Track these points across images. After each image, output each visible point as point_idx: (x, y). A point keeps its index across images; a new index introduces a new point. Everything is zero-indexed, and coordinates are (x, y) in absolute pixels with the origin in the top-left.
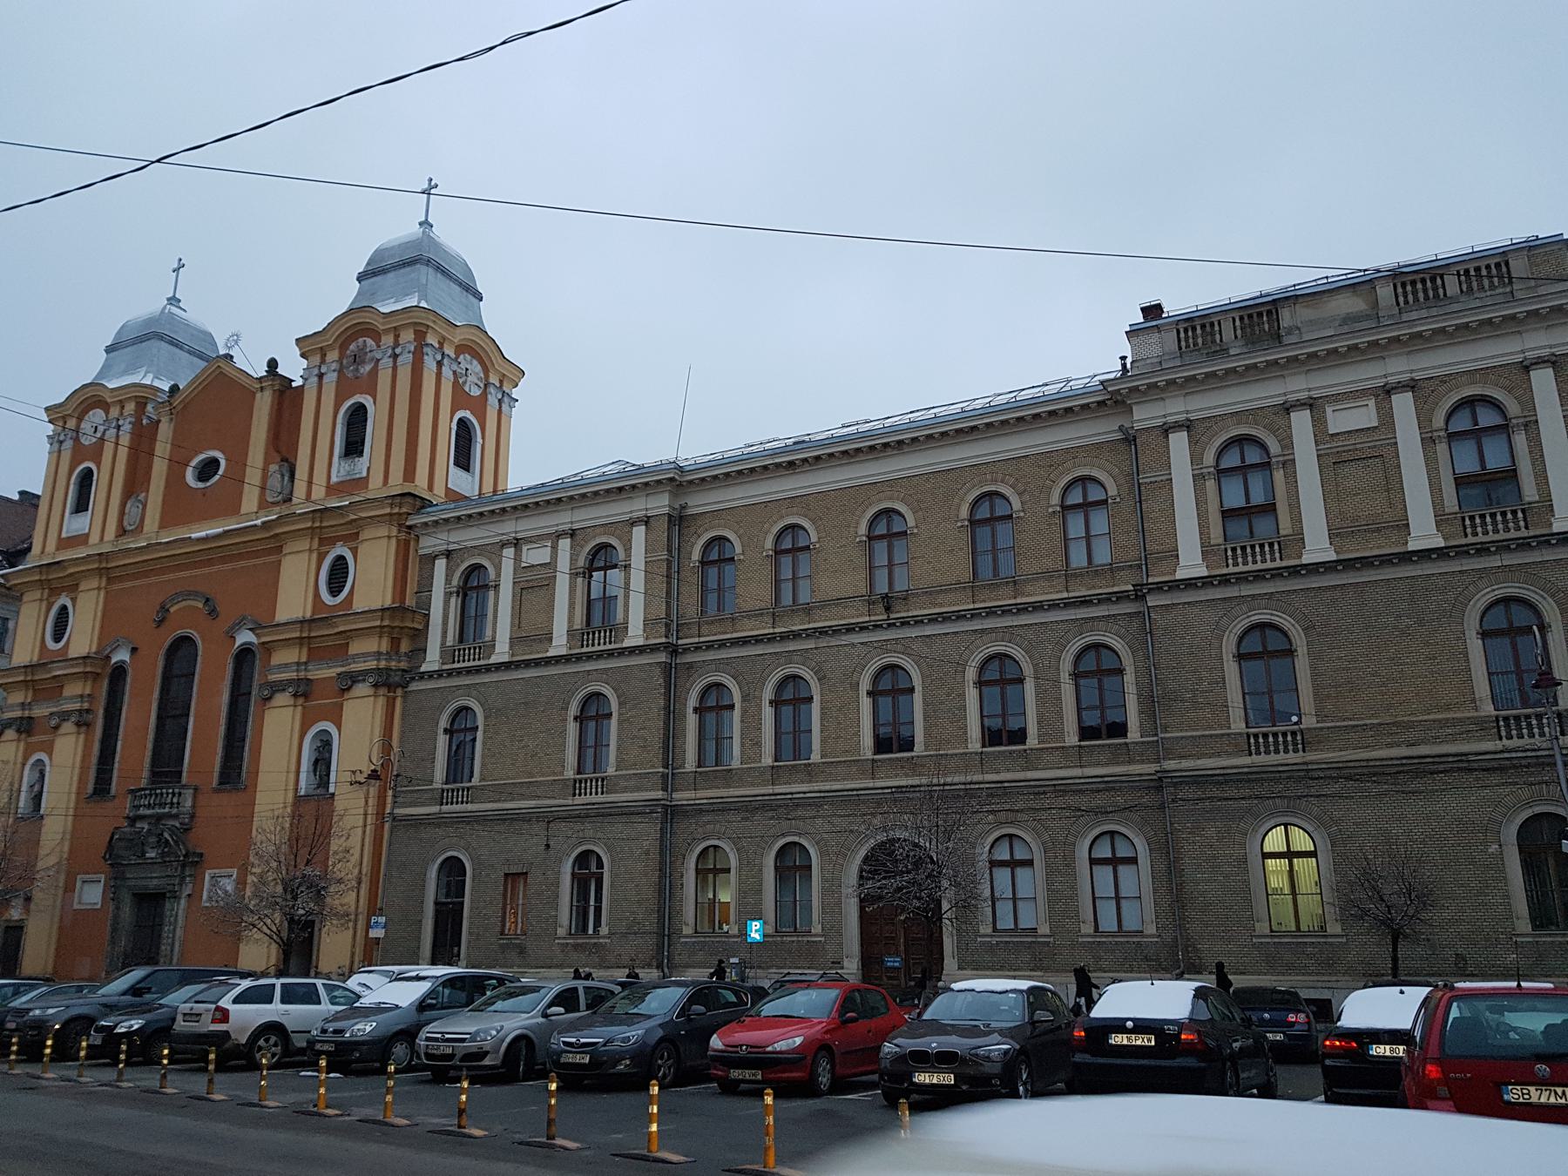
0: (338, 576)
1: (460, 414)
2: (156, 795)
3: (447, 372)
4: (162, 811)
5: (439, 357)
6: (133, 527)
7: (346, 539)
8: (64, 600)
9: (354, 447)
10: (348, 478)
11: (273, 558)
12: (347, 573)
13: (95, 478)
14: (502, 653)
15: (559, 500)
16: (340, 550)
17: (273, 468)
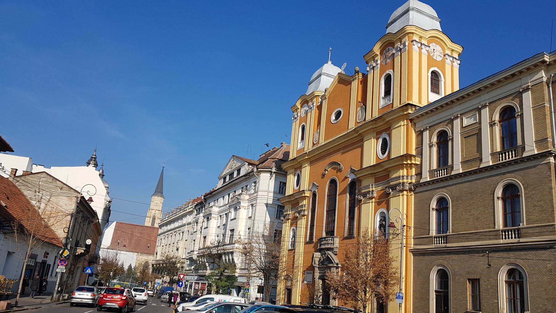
0: (385, 147)
1: (432, 69)
2: (326, 240)
3: (424, 51)
4: (328, 246)
5: (419, 45)
6: (316, 142)
7: (385, 130)
8: (298, 172)
9: (388, 92)
10: (385, 105)
11: (361, 144)
12: (387, 144)
13: (305, 128)
14: (458, 169)
15: (480, 90)
16: (385, 135)
17: (359, 109)
